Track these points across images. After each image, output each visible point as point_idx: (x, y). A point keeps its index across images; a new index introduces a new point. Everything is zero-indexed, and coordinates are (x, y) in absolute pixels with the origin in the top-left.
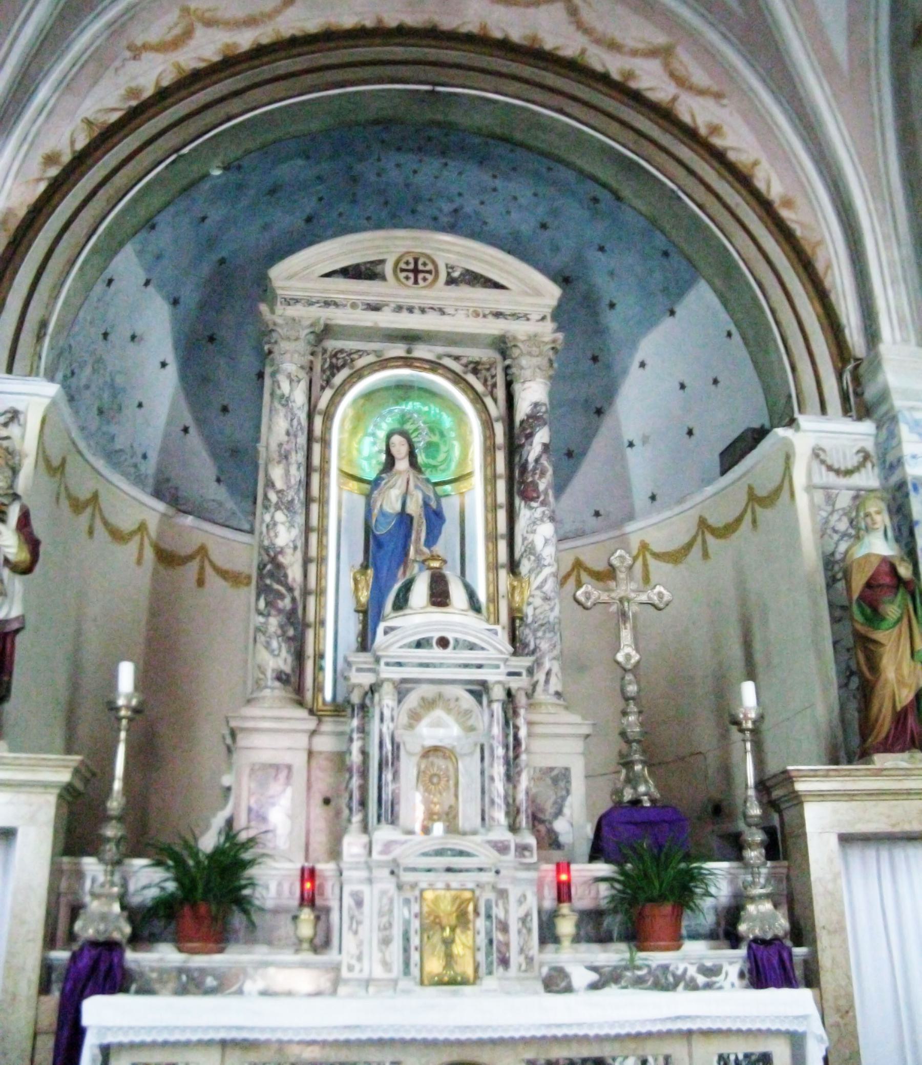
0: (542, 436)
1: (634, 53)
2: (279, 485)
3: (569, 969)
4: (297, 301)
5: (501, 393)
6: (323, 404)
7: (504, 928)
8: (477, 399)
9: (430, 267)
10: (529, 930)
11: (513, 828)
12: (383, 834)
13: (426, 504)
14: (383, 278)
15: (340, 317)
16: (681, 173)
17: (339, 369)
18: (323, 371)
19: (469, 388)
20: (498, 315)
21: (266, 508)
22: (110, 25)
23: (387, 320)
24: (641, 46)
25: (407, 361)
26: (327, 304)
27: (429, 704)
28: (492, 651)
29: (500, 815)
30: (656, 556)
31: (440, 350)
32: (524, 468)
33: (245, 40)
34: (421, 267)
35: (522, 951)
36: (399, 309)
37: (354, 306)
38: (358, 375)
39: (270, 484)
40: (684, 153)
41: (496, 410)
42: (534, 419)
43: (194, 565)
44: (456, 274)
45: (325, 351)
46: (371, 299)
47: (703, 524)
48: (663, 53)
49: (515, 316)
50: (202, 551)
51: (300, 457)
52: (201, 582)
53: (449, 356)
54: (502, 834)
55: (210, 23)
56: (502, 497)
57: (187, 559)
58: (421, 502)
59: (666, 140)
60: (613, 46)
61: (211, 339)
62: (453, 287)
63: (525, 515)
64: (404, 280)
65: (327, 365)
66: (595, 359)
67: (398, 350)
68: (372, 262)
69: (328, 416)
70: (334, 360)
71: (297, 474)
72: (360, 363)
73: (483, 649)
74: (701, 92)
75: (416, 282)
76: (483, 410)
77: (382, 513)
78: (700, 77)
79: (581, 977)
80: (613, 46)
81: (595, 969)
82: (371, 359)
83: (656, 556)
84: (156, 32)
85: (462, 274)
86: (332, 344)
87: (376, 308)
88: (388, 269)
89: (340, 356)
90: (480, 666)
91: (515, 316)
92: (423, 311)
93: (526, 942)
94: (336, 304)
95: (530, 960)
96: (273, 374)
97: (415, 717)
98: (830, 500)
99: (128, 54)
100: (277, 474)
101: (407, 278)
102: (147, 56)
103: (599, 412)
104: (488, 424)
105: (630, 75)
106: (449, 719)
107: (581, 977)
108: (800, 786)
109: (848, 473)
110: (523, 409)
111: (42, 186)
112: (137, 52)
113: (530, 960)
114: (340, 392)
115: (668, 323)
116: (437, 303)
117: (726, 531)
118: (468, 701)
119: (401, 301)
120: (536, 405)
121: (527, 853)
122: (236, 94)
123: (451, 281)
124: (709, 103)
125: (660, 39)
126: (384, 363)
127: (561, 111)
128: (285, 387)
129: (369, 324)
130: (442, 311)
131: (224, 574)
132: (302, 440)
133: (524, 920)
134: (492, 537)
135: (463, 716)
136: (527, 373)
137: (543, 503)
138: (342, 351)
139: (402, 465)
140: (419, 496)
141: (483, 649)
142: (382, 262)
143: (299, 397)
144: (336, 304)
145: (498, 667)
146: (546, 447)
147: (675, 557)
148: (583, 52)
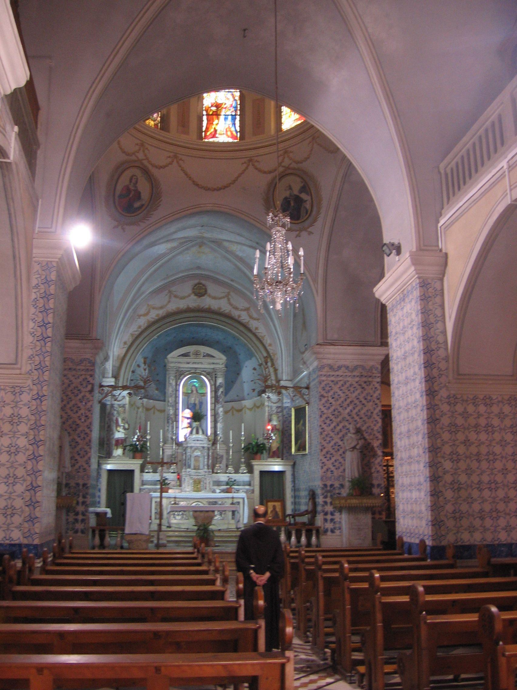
0: (221, 390)
1: (242, 310)
2: (171, 402)
4: (173, 362)
5: (214, 379)
6: (178, 383)
7: (206, 484)
8: (209, 381)
11: (208, 469)
12: (188, 470)
16: (249, 340)
19: (207, 378)
20: (213, 363)
21: (168, 406)
22: (133, 310)
24: (243, 308)
26: (179, 363)
27: (196, 449)
29: (206, 467)
30: (248, 408)
32: (217, 397)
33: (161, 312)
37: (184, 363)
38: (185, 377)
39: (169, 402)
40: (250, 335)
41: (213, 383)
42: (220, 386)
43: (152, 410)
47: (255, 405)
48: (247, 309)
49: (217, 364)
50: (154, 407)
51: (174, 396)
52: (154, 413)
54: (206, 470)
55: (154, 308)
56: (213, 402)
57: (151, 409)
59: (246, 332)
60: (236, 308)
61: (154, 361)
63: (217, 406)
66: (237, 363)
69: (179, 385)
71: (174, 399)
74: (255, 319)
76: (210, 383)
78: (255, 315)
79: (218, 491)
80: (236, 308)
81: (220, 490)
83: (248, 408)
84: (142, 311)
87: (188, 363)
88: (191, 354)
91: (217, 364)
96: (169, 378)
97: (194, 451)
98: (271, 408)
99: (137, 317)
100: (170, 399)
102: (142, 317)
103: (238, 374)
104: (211, 386)
105: (239, 316)
106: (199, 451)
107: (218, 491)
108: (253, 463)
109: (275, 403)
110: (218, 384)
111: (124, 350)
112: (140, 316)
115: (250, 361)
117: (258, 407)
118: (202, 449)
120: (220, 383)
122: (159, 327)
123: (204, 356)
124: (256, 322)
125: (247, 305)
127: (225, 326)
128: (171, 381)
130: (201, 363)
131: (158, 410)
132: (175, 392)
133: (209, 482)
134: (211, 410)
135: (201, 451)
136: (218, 376)
137: (221, 404)
139: (195, 392)
142: (189, 352)
143: (174, 383)
146: (222, 392)
147: (250, 409)
148: (230, 310)
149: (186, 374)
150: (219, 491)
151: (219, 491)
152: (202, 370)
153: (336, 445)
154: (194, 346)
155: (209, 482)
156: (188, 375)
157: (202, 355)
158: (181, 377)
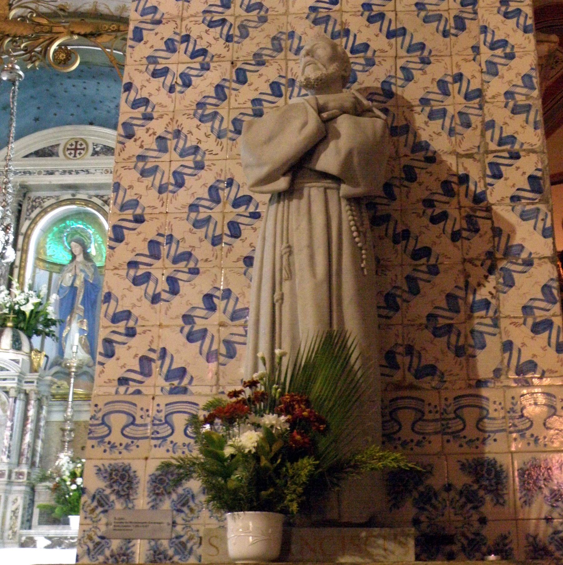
3: (36, 538)
6: (23, 230)
9: (84, 146)
10: (17, 517)
13: (86, 281)
14: (58, 156)
15: (31, 180)
17: (36, 208)
18: (28, 210)
23: (57, 179)
25: (72, 201)
26: (25, 173)
28: (13, 371)
31: (92, 193)
34: (73, 147)
35: (11, 528)
36: (64, 172)
37: (39, 173)
38: (45, 211)
44: (98, 149)
45: (30, 198)
46: (49, 168)
53: (97, 196)
58: (82, 280)
62: (96, 156)
64: (68, 156)
65: (29, 207)
67: (67, 195)
68: (52, 146)
69: (27, 236)
70: (34, 204)
72: (47, 204)
73: (8, 370)
75: (75, 156)
77: (61, 287)
79: (42, 542)
81: (49, 538)
82: (53, 201)
85: (102, 149)
86: (33, 195)
87: (51, 173)
89: (37, 200)
90: (5, 380)
92: (77, 173)
93: (14, 524)
94: (30, 173)
95: (14, 533)
101: (70, 154)
113: (14, 533)
114: (34, 222)
116: (85, 167)
119: (65, 168)
121: (21, 477)
123: (95, 153)
126: (59, 203)
129: (48, 183)
130: (88, 172)
138: (39, 198)
140: (83, 275)
141: (8, 370)
142: (58, 145)
144: (30, 173)
145: (14, 379)
149: (47, 204)
150: (49, 542)
151: (49, 542)
152: (92, 193)
153: (216, 200)
154: (68, 128)
155: (14, 512)
156: (52, 207)
157: (91, 151)
158: (33, 215)
